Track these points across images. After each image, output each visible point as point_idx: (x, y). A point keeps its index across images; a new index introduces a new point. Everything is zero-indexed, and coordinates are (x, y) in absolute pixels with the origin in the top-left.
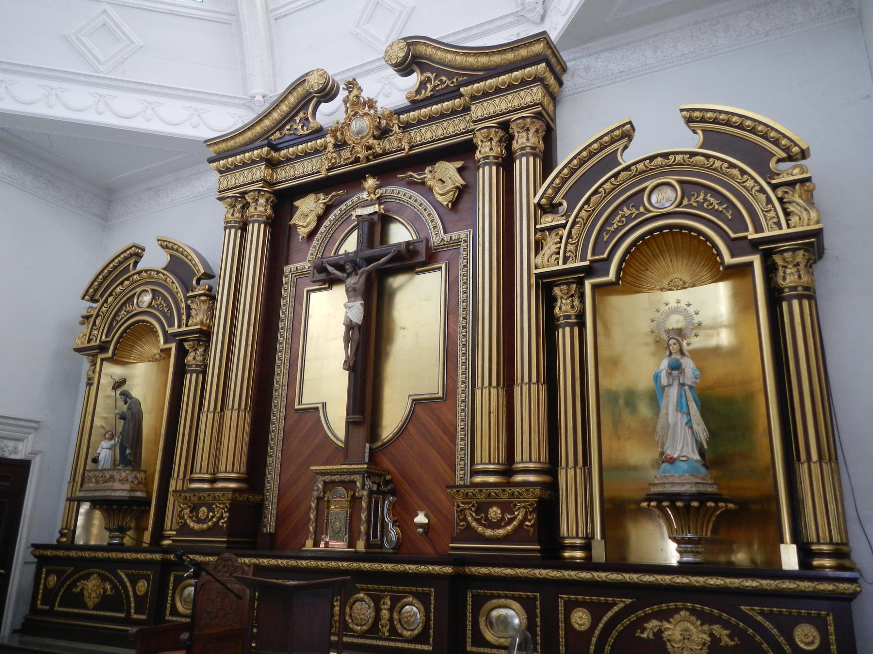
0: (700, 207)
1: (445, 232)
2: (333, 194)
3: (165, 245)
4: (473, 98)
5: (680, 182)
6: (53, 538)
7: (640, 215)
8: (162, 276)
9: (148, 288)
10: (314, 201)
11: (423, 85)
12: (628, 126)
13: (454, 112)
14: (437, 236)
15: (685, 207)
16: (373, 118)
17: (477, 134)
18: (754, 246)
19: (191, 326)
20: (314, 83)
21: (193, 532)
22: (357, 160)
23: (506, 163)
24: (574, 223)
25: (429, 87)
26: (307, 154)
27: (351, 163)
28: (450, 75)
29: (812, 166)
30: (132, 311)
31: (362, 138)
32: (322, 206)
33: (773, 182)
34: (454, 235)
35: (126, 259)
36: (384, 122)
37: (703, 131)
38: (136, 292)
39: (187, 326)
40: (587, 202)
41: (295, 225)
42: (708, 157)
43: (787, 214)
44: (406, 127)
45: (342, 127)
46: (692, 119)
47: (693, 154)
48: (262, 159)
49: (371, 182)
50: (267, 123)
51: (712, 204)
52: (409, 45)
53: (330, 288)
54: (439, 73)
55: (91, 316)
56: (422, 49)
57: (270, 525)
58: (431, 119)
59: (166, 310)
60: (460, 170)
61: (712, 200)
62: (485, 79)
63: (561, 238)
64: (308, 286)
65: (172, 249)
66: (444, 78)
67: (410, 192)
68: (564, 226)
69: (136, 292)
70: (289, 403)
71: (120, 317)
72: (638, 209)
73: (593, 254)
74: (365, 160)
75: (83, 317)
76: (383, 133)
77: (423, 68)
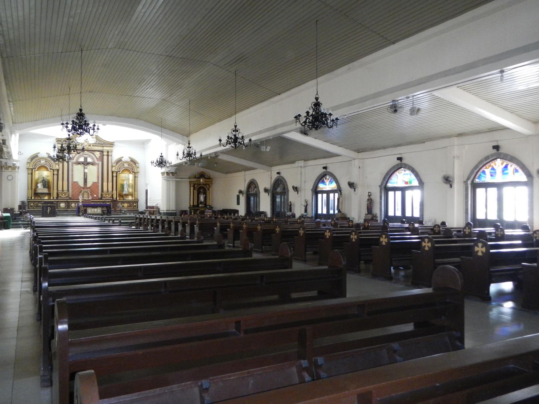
3: (47, 154)
6: (27, 198)
11: (96, 142)
14: (96, 162)
18: (134, 172)
21: (62, 197)
23: (108, 156)
25: (98, 142)
29: (140, 165)
34: (99, 162)
44: (93, 146)
46: (130, 158)
54: (99, 141)
57: (70, 196)
58: (97, 146)
70: (72, 181)
76: (90, 146)
77: (97, 139)
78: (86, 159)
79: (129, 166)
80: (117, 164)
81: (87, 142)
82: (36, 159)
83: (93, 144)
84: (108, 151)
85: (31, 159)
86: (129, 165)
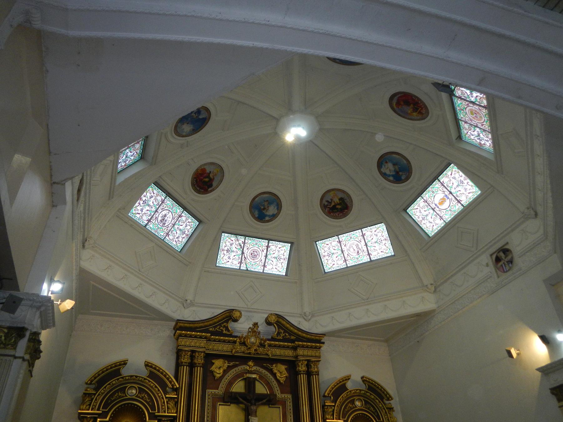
0: (369, 409)
1: (282, 393)
2: (234, 363)
4: (299, 346)
5: (364, 400)
7: (354, 408)
8: (148, 382)
9: (136, 386)
10: (221, 363)
11: (279, 334)
12: (350, 377)
13: (288, 347)
15: (365, 408)
16: (260, 339)
17: (301, 361)
19: (169, 413)
20: (236, 314)
22: (250, 353)
23: (309, 374)
24: (337, 406)
25: (282, 335)
26: (224, 341)
27: (246, 353)
28: (290, 335)
30: (123, 397)
31: (255, 345)
32: (227, 366)
33: (387, 407)
34: (286, 395)
35: (120, 365)
36: (263, 342)
37: (367, 385)
38: (128, 386)
39: (167, 413)
40: (340, 400)
41: (213, 371)
42: (371, 394)
43: (390, 417)
44: (270, 345)
45: (245, 337)
46: (364, 380)
47: (367, 392)
48: (206, 338)
49: (251, 363)
50: (211, 322)
51: (371, 409)
52: (277, 317)
53: (230, 405)
54: (285, 332)
55: (95, 394)
56: (280, 320)
58: (280, 347)
59: (148, 401)
60: (286, 369)
61: (371, 408)
62: (305, 342)
63: (334, 410)
64: (219, 402)
65: (155, 369)
66: (287, 334)
67: (267, 373)
68: (334, 406)
69: (128, 386)
71: (114, 398)
72: (353, 405)
73: (342, 418)
74: (253, 354)
75: (84, 393)
77: (279, 327)
78: (250, 384)
79: (368, 406)
80: (335, 401)
81: (255, 332)
82: (114, 381)
83: (269, 340)
84: (309, 361)
85: (97, 382)
86: (366, 402)
